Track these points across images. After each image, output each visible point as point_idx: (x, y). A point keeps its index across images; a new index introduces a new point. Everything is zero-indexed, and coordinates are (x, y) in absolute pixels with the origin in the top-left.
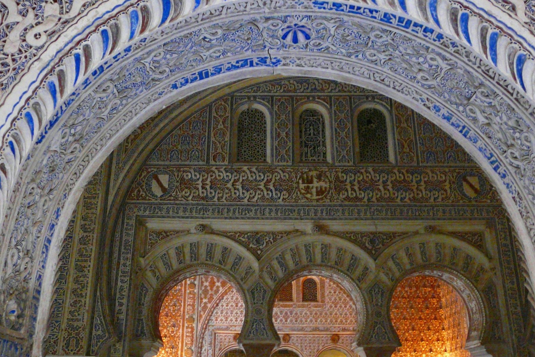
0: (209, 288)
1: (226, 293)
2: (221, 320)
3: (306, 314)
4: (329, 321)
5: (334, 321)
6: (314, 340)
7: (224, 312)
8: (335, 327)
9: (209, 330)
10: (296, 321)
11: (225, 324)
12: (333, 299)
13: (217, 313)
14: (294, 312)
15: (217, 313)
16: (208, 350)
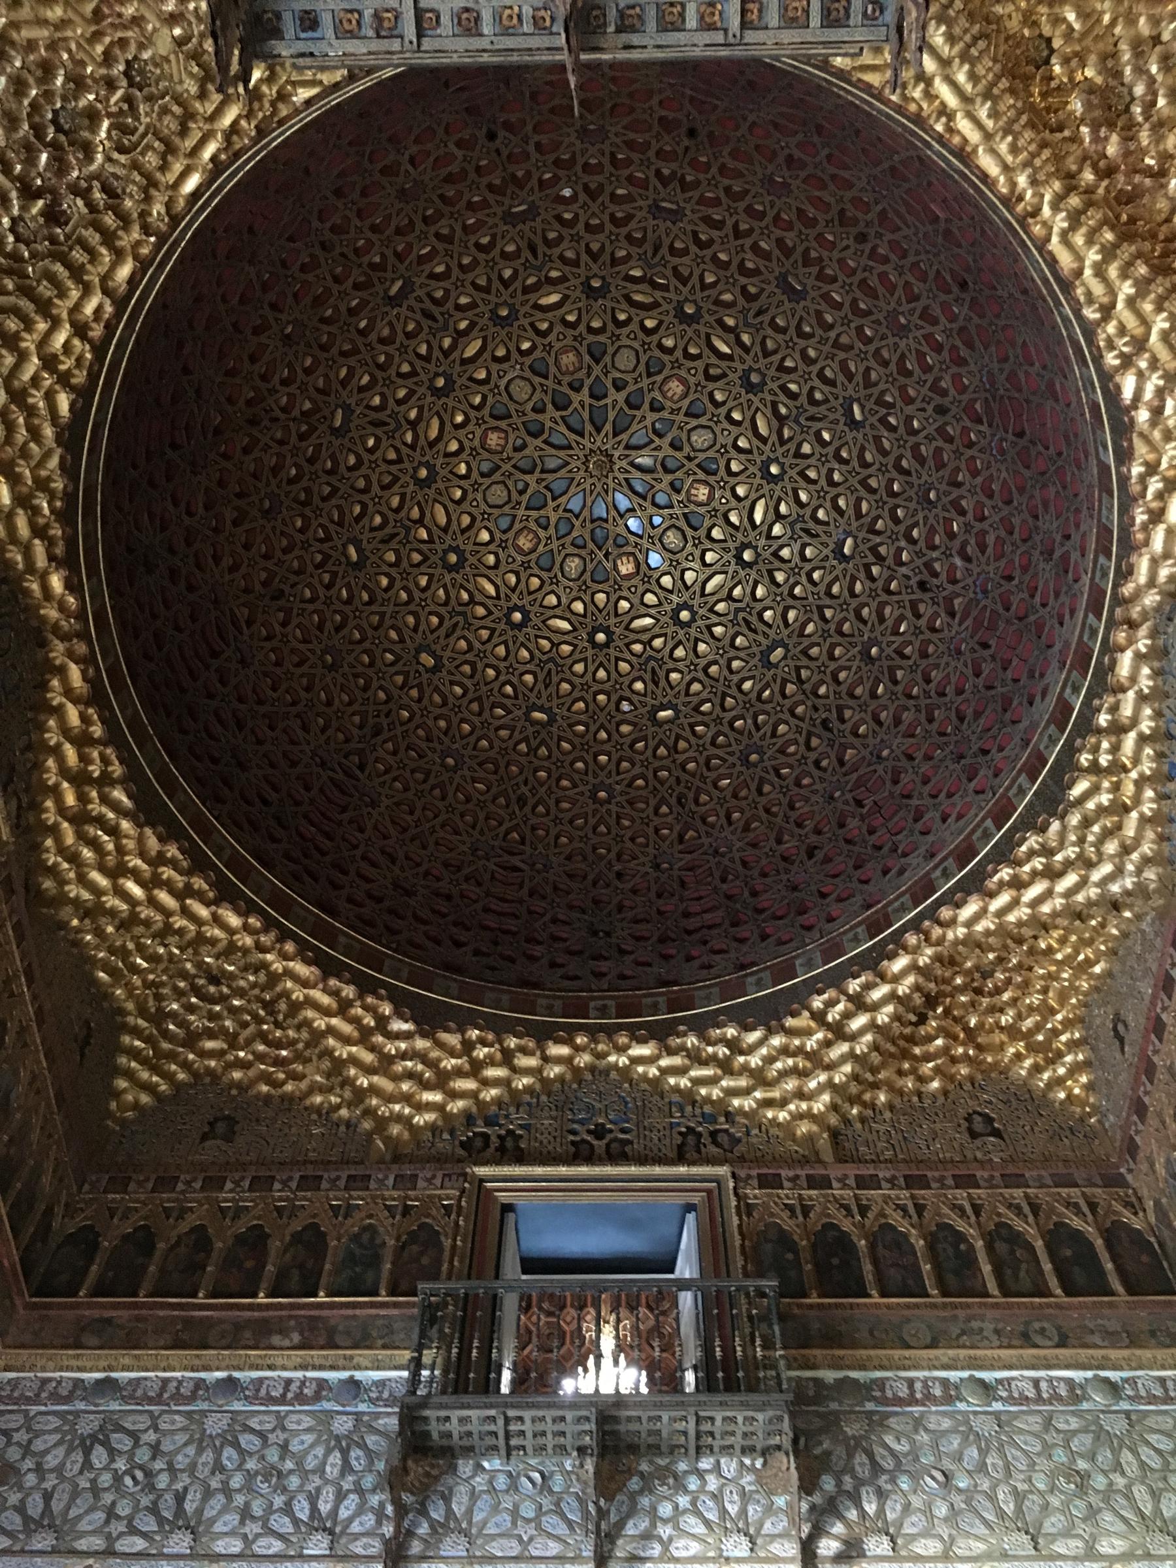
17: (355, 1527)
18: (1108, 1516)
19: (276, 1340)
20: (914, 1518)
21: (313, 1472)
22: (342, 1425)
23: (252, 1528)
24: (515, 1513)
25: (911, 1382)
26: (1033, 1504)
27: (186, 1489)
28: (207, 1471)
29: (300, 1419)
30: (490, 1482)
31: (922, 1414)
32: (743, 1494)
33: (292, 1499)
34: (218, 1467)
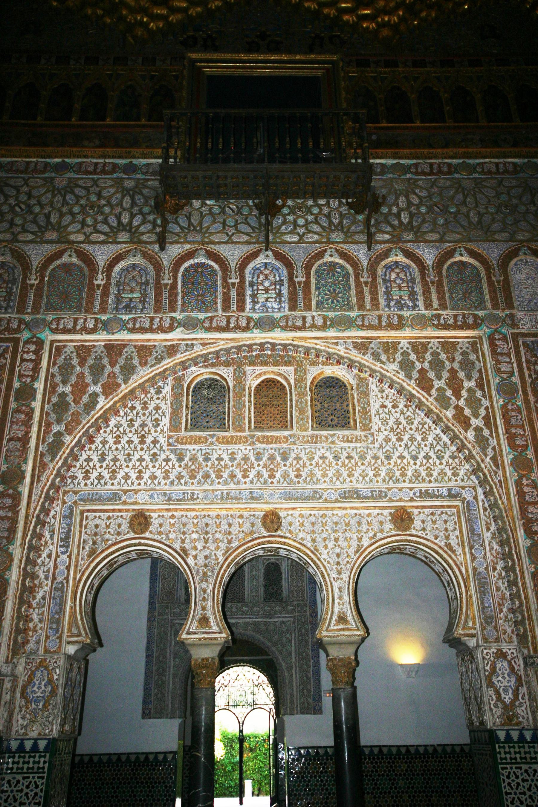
0: (70, 399)
1: (114, 410)
2: (100, 477)
3: (323, 457)
4: (383, 474)
5: (398, 474)
6: (347, 525)
7: (108, 458)
8: (400, 490)
9: (64, 502)
10: (298, 476)
11: (109, 487)
12: (391, 422)
13: (89, 460)
14: (293, 455)
15: (89, 460)
16: (57, 556)
17: (142, 229)
18: (523, 223)
19: (86, 143)
20: (427, 225)
21: (117, 205)
22: (129, 184)
23: (88, 230)
24: (224, 224)
25: (431, 165)
26: (487, 218)
27: (50, 213)
28: (59, 205)
29: (105, 181)
30: (211, 209)
31: (436, 179)
32: (341, 214)
33: (107, 217)
34: (65, 202)
